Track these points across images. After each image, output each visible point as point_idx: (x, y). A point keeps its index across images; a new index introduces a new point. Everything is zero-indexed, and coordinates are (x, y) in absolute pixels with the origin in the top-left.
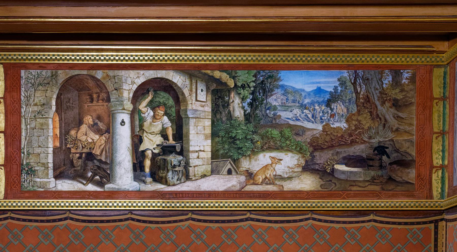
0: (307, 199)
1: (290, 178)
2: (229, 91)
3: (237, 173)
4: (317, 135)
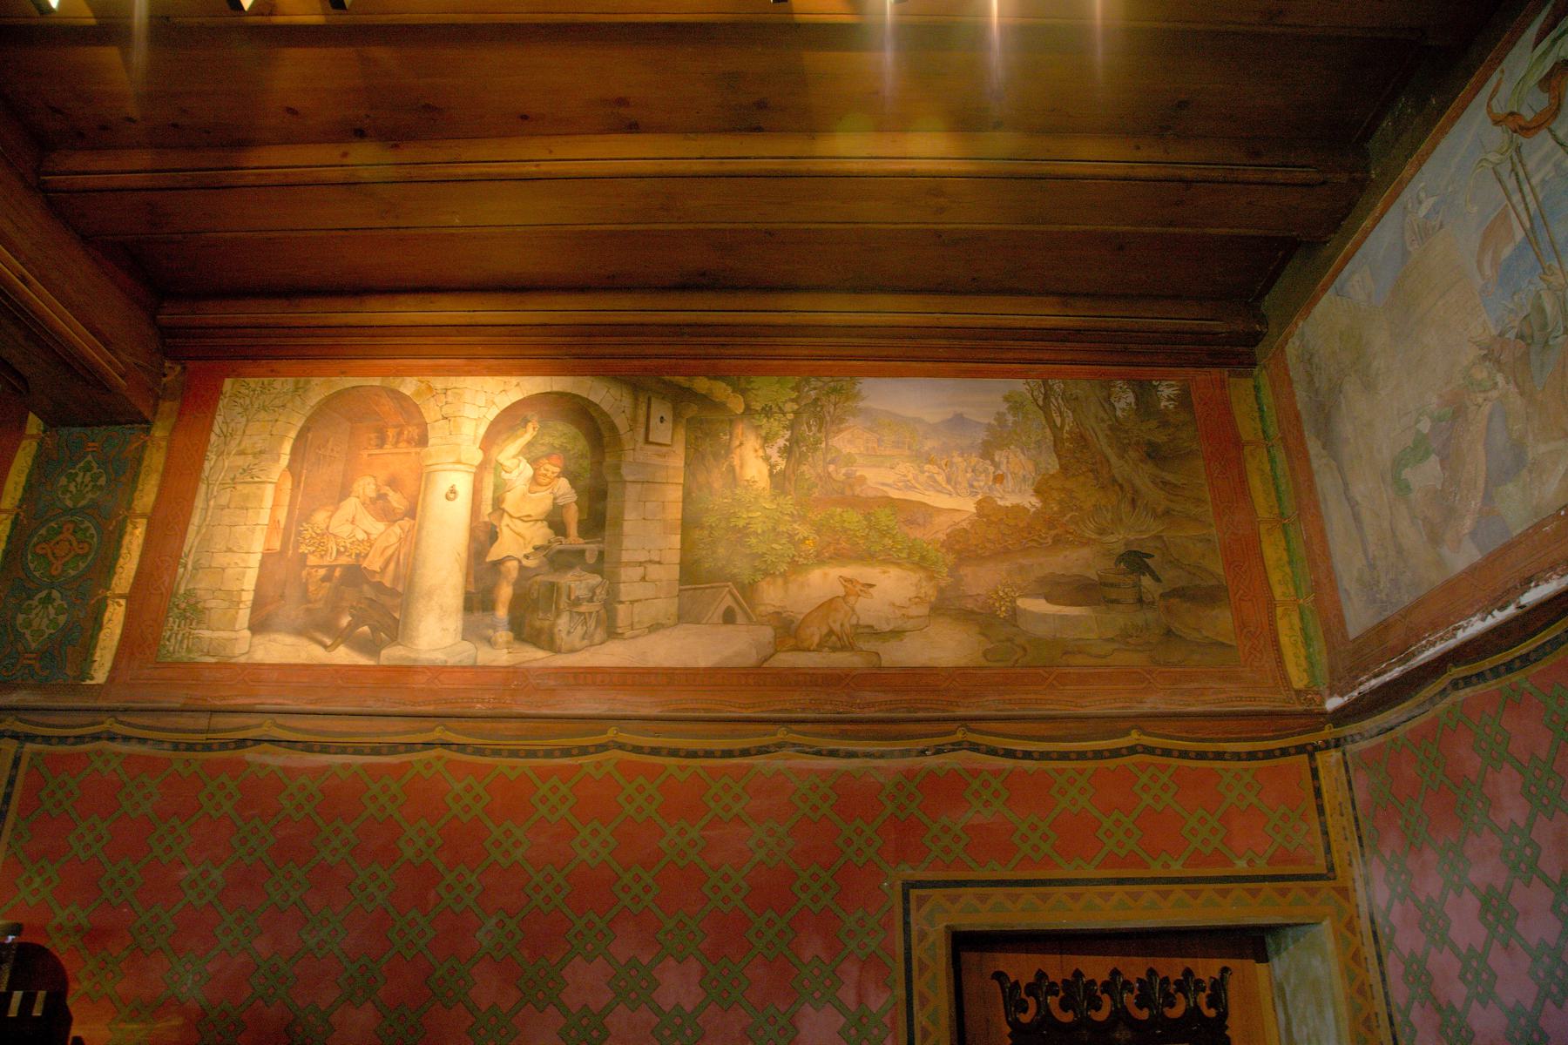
3: (749, 618)
4: (964, 525)
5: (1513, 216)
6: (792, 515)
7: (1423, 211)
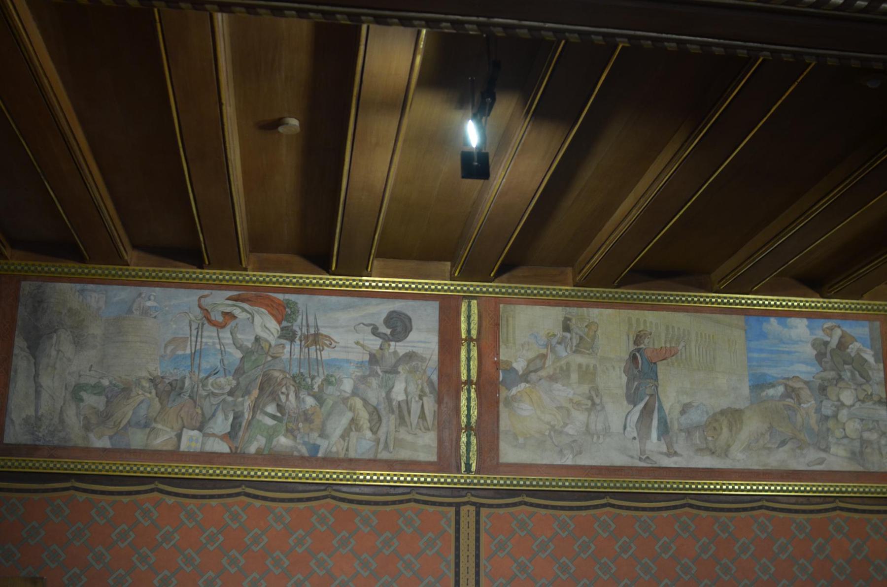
7: (149, 304)
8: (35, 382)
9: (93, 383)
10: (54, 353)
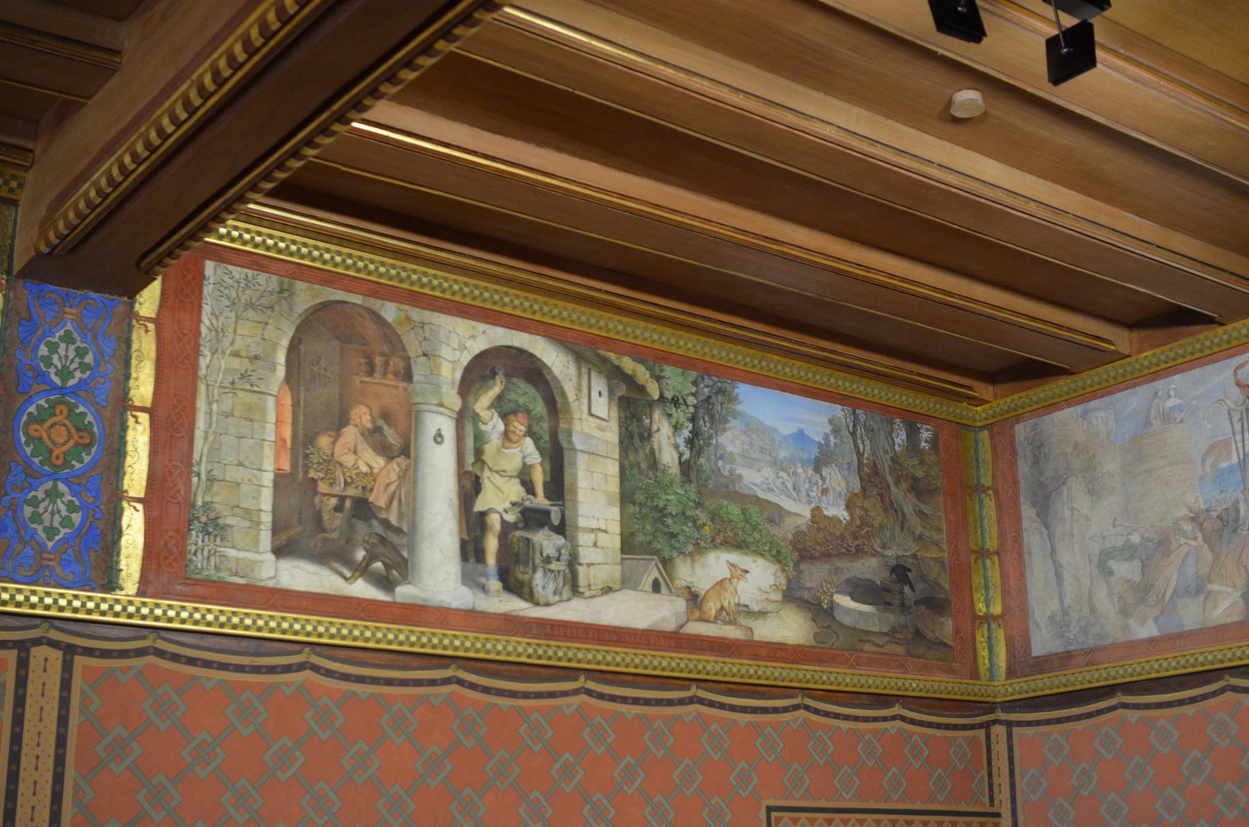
0: (793, 662)
1: (762, 614)
2: (651, 404)
3: (670, 590)
4: (804, 528)
5: (1234, 446)
6: (694, 501)
7: (1170, 403)
8: (1054, 562)
9: (1120, 545)
10: (1067, 513)
